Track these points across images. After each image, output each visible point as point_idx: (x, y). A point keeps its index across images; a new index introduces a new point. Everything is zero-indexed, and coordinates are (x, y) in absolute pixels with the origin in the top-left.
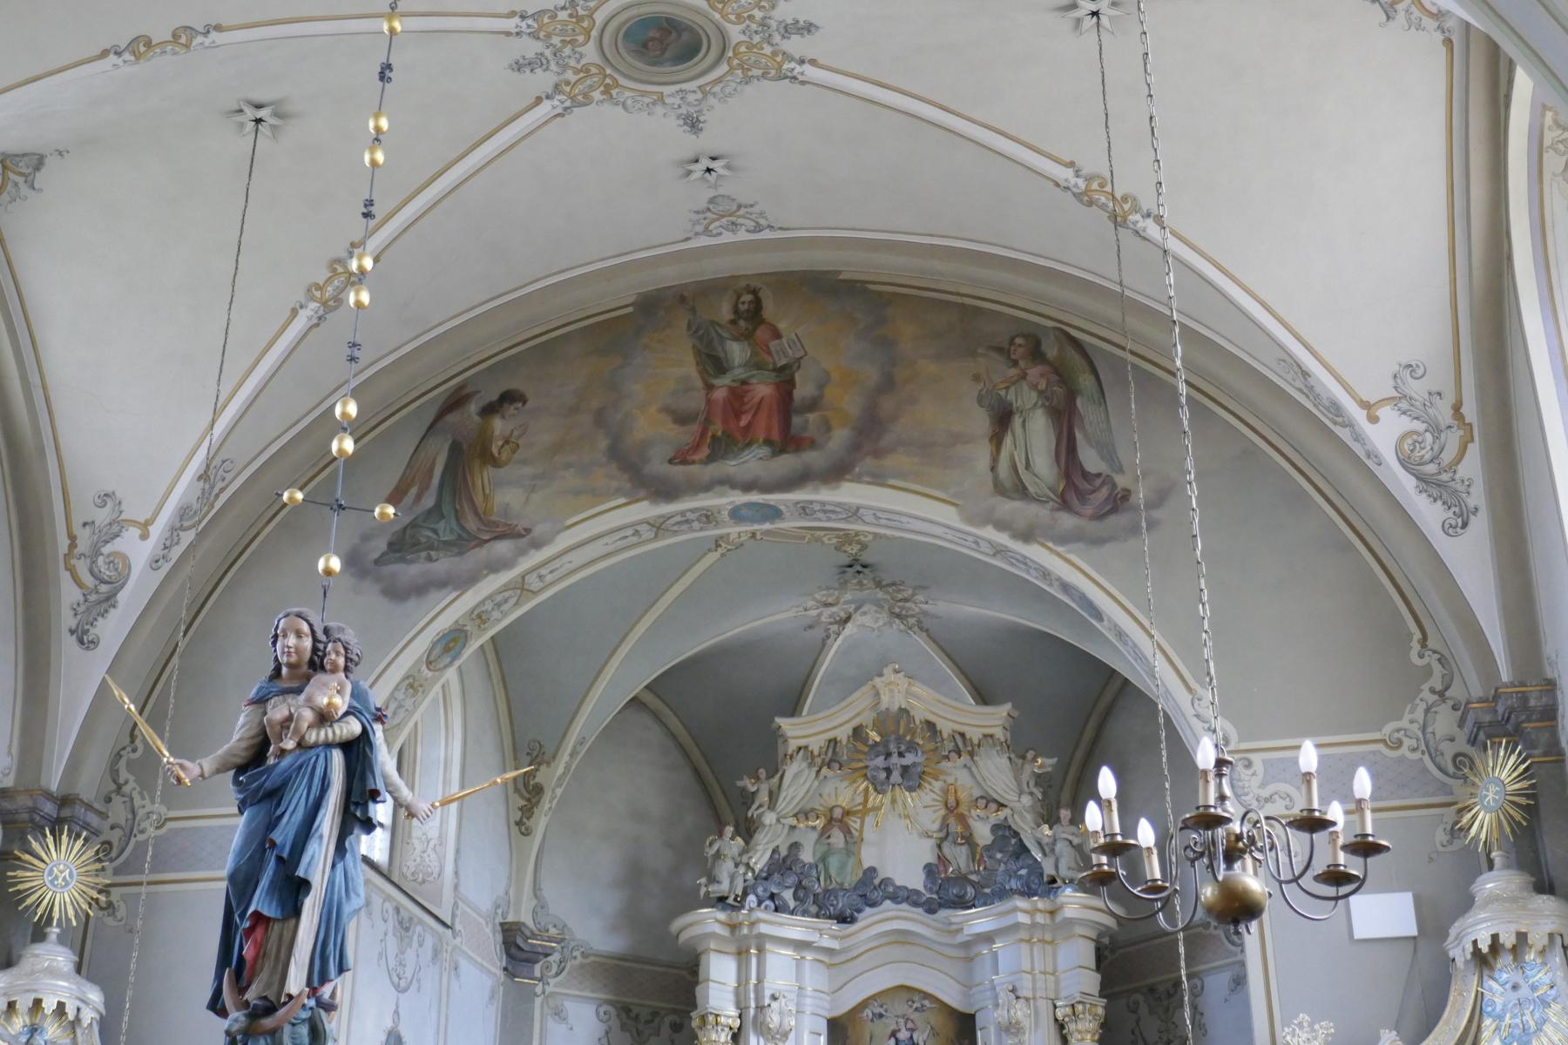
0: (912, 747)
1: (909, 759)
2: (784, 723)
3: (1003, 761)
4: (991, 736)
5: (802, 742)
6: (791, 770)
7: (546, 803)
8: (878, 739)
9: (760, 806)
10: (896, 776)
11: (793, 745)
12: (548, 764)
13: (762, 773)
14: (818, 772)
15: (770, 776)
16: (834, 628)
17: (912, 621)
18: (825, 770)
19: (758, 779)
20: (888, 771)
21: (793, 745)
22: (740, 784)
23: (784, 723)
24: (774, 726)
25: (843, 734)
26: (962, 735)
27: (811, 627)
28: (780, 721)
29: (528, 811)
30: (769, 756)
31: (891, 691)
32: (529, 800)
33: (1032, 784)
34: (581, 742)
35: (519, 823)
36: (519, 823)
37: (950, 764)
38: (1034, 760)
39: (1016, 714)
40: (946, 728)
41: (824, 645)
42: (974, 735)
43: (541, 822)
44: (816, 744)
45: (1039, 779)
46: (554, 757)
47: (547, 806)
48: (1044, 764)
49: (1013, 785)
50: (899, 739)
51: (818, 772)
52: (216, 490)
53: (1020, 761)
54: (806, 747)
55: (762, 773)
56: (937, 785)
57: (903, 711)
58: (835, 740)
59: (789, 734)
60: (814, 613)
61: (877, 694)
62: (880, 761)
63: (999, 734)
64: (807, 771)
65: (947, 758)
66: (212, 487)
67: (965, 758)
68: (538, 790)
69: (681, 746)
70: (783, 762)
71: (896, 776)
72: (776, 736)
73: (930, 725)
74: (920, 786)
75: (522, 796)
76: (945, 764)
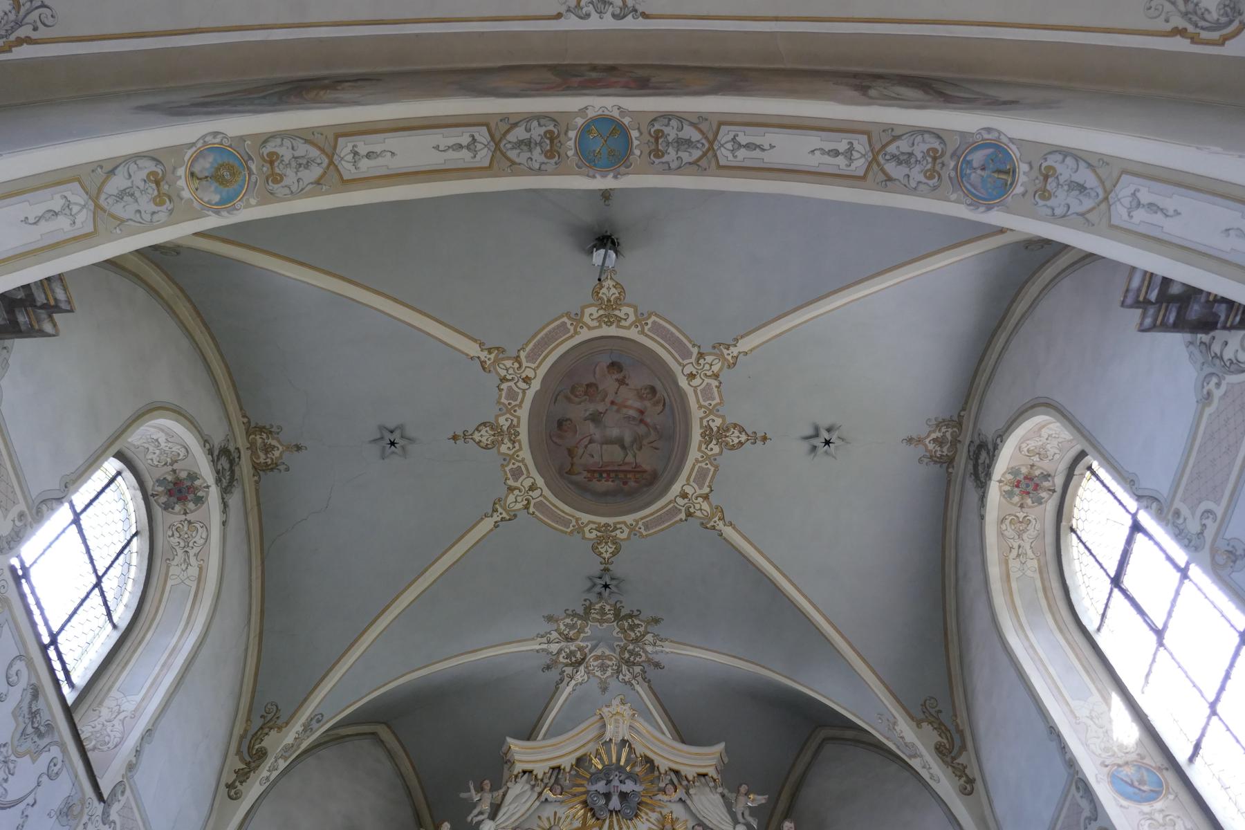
0: (633, 777)
1: (628, 787)
2: (515, 745)
3: (717, 798)
4: (704, 775)
5: (528, 767)
6: (517, 789)
7: (265, 772)
8: (600, 767)
9: (481, 813)
10: (615, 803)
11: (519, 767)
12: (280, 729)
13: (487, 785)
14: (540, 794)
15: (493, 789)
16: (569, 670)
17: (637, 669)
18: (547, 793)
19: (480, 789)
20: (608, 796)
21: (519, 767)
22: (463, 795)
23: (515, 745)
24: (504, 749)
25: (567, 763)
26: (677, 772)
27: (548, 667)
28: (509, 740)
29: (243, 776)
30: (496, 771)
31: (617, 721)
32: (248, 764)
33: (747, 813)
34: (318, 718)
35: (229, 786)
36: (229, 786)
37: (665, 798)
38: (747, 794)
39: (726, 760)
40: (663, 764)
41: (557, 689)
42: (690, 772)
43: (253, 789)
44: (540, 769)
45: (753, 811)
46: (287, 724)
47: (265, 774)
48: (757, 800)
49: (728, 818)
50: (620, 769)
51: (540, 794)
52: (22, 32)
53: (732, 796)
54: (531, 772)
55: (487, 785)
56: (654, 816)
57: (624, 742)
58: (559, 768)
59: (517, 757)
60: (554, 648)
61: (604, 726)
62: (601, 786)
63: (712, 772)
64: (529, 793)
65: (664, 791)
66: (19, 24)
67: (680, 793)
68: (262, 754)
69: (409, 793)
70: (509, 780)
71: (615, 803)
72: (505, 761)
73: (649, 761)
74: (636, 816)
75: (242, 760)
76: (660, 796)
